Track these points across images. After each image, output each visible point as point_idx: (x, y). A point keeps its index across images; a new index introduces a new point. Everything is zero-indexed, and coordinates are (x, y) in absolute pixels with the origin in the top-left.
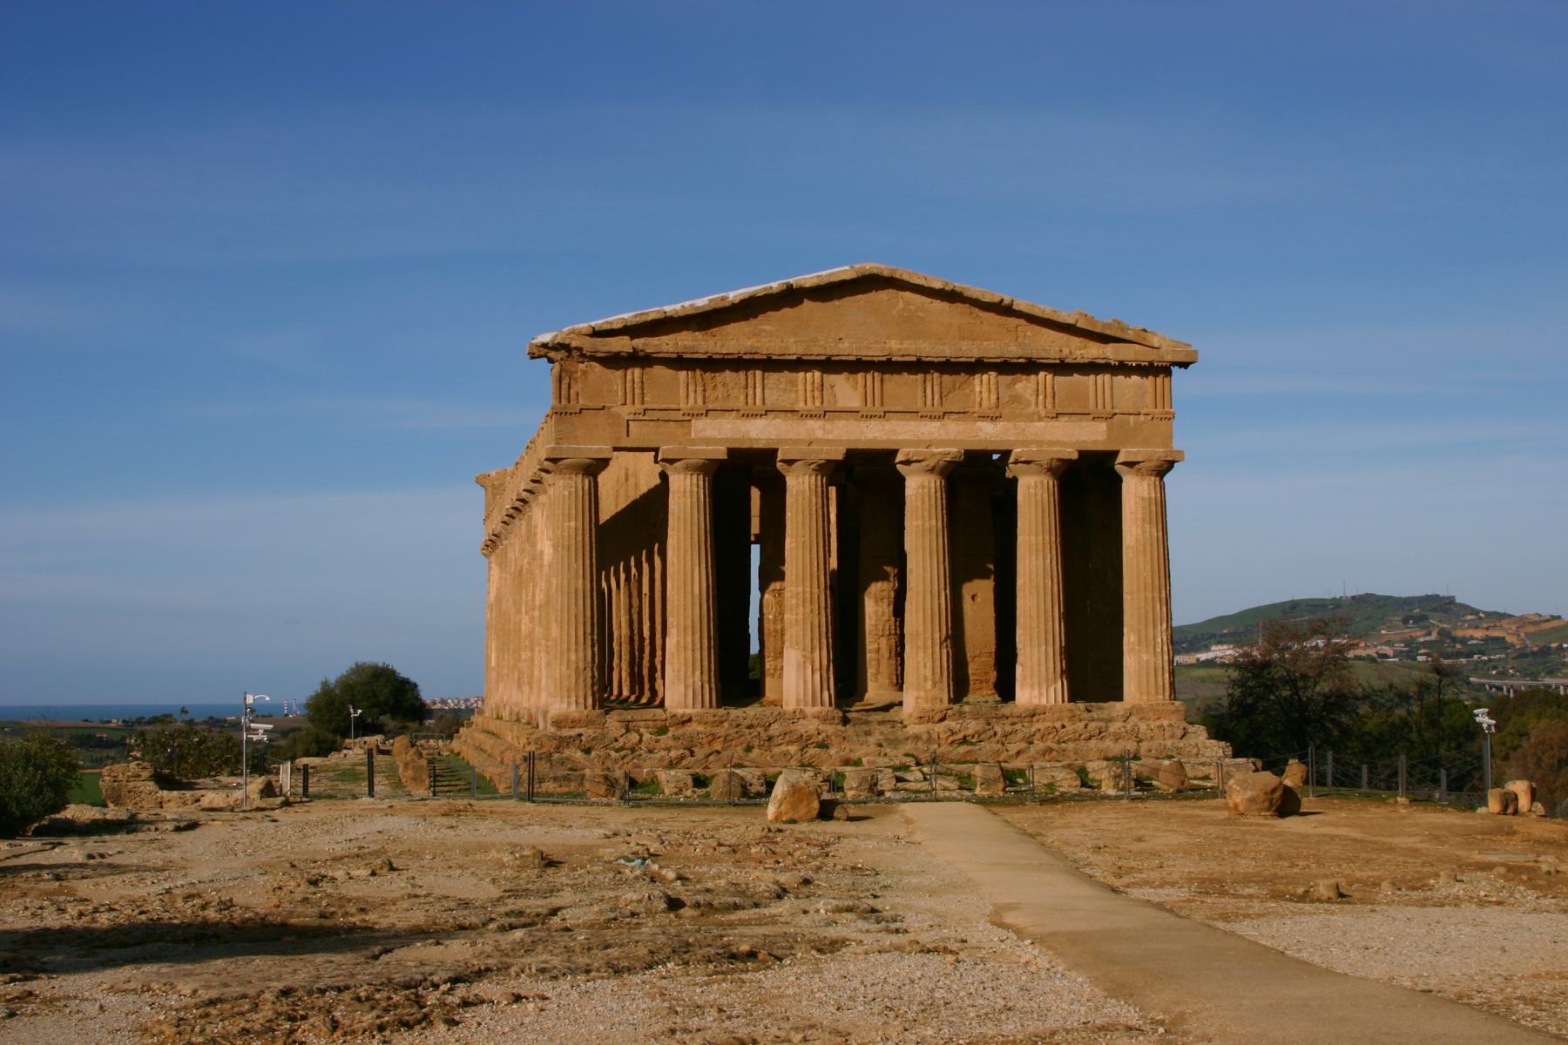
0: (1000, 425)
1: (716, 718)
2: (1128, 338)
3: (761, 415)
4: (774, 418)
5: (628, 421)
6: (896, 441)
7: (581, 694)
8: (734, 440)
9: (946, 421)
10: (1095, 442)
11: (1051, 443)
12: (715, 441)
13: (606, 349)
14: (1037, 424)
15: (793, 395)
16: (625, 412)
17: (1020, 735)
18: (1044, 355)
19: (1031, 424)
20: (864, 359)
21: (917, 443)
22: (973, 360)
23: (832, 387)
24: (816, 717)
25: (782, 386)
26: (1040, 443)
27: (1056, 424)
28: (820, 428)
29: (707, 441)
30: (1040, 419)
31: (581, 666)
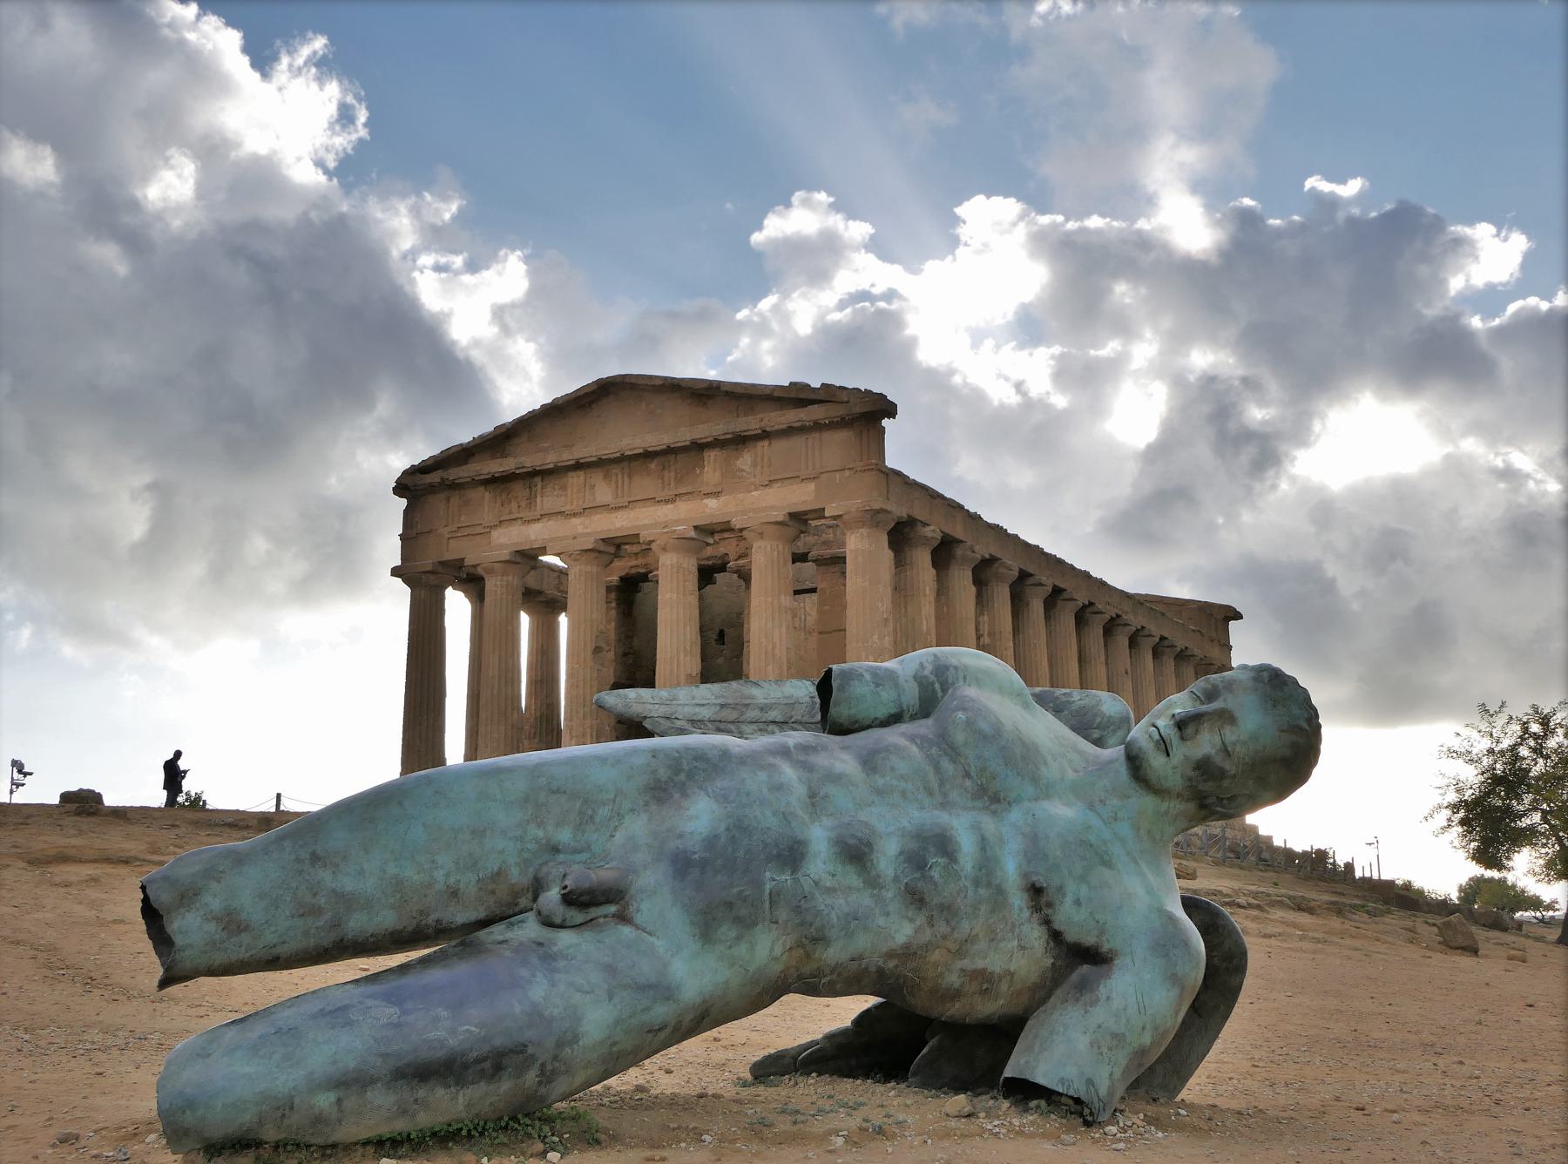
2: (819, 397)
3: (538, 519)
4: (548, 521)
5: (449, 538)
9: (678, 503)
13: (421, 482)
14: (753, 493)
19: (749, 494)
20: (604, 457)
22: (688, 443)
25: (555, 493)
27: (771, 490)
28: (581, 524)
30: (756, 489)
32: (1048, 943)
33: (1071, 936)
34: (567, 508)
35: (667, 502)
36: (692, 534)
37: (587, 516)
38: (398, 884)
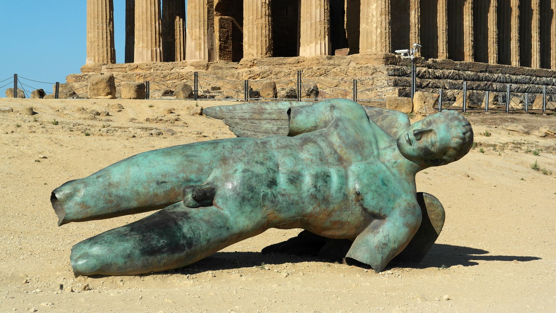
1: (147, 67)
7: (92, 54)
17: (283, 74)
31: (93, 40)
32: (362, 212)
33: (370, 209)
38: (138, 193)
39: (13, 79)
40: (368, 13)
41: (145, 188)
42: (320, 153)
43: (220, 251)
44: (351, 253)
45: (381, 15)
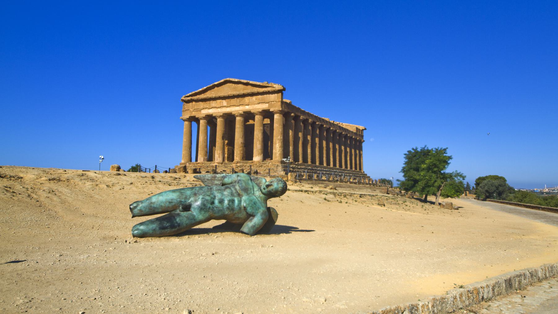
0: (249, 106)
6: (232, 111)
8: (207, 113)
10: (266, 108)
11: (258, 109)
12: (204, 114)
15: (216, 104)
16: (191, 110)
18: (254, 91)
21: (235, 111)
23: (223, 102)
24: (217, 163)
26: (256, 109)
29: (203, 114)
30: (256, 104)
33: (249, 213)
34: (217, 106)
35: (238, 106)
36: (243, 113)
37: (222, 108)
38: (161, 206)
39: (155, 167)
40: (276, 147)
41: (164, 204)
42: (231, 192)
43: (192, 228)
44: (242, 229)
45: (280, 147)
